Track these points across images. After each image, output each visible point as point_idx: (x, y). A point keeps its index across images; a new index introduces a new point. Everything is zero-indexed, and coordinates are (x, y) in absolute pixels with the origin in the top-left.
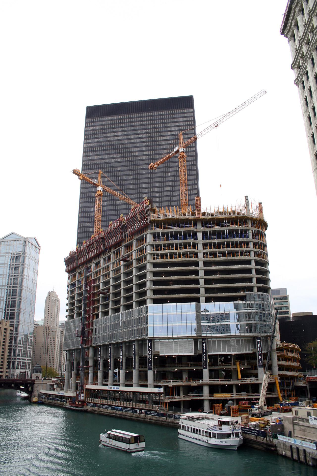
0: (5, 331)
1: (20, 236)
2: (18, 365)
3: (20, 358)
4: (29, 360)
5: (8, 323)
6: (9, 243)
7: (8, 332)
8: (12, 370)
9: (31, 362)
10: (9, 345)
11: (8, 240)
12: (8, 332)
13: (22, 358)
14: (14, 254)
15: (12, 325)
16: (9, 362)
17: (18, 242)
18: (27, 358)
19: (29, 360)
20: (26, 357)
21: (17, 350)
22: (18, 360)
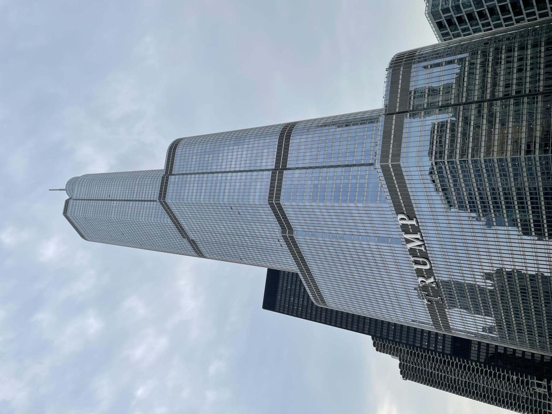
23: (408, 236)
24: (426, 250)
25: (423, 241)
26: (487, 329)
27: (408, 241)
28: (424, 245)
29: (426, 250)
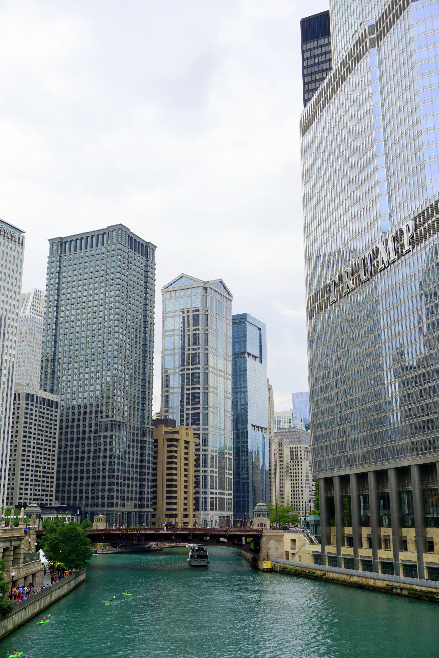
0: (186, 445)
1: (196, 280)
2: (212, 503)
3: (214, 491)
4: (230, 494)
5: (191, 432)
6: (178, 293)
7: (192, 447)
8: (202, 512)
9: (232, 497)
10: (195, 469)
11: (176, 289)
12: (192, 447)
13: (218, 491)
14: (189, 312)
15: (196, 435)
16: (197, 499)
17: (194, 291)
18: (225, 492)
19: (230, 494)
20: (224, 489)
21: (209, 478)
22: (212, 496)
23: (390, 242)
24: (380, 271)
25: (389, 265)
26: (402, 349)
27: (386, 243)
28: (385, 267)
29: (380, 271)
